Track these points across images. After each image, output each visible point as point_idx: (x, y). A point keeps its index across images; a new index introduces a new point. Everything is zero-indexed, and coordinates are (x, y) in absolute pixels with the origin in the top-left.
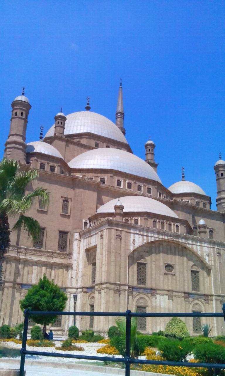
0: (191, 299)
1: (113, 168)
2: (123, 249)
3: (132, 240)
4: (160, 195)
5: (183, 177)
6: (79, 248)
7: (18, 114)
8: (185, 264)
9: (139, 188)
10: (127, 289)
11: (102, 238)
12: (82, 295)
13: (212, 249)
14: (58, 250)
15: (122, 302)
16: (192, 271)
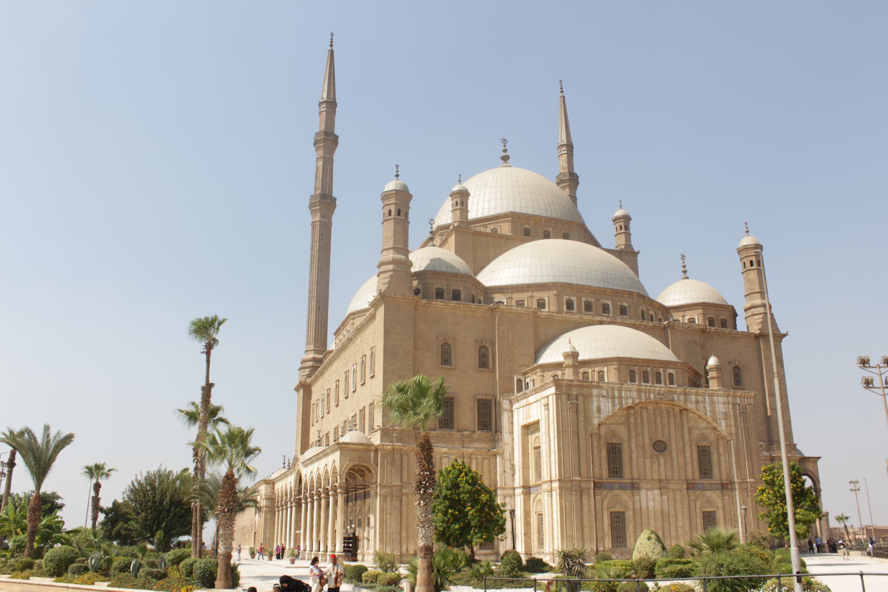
0: (698, 492)
1: (557, 280)
2: (581, 425)
3: (594, 406)
4: (643, 318)
5: (685, 272)
6: (512, 423)
7: (393, 213)
8: (686, 436)
9: (605, 309)
10: (592, 486)
11: (548, 409)
12: (524, 499)
13: (731, 406)
14: (479, 429)
15: (586, 507)
16: (698, 447)
